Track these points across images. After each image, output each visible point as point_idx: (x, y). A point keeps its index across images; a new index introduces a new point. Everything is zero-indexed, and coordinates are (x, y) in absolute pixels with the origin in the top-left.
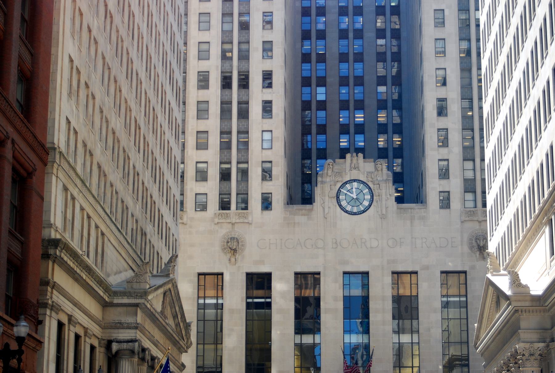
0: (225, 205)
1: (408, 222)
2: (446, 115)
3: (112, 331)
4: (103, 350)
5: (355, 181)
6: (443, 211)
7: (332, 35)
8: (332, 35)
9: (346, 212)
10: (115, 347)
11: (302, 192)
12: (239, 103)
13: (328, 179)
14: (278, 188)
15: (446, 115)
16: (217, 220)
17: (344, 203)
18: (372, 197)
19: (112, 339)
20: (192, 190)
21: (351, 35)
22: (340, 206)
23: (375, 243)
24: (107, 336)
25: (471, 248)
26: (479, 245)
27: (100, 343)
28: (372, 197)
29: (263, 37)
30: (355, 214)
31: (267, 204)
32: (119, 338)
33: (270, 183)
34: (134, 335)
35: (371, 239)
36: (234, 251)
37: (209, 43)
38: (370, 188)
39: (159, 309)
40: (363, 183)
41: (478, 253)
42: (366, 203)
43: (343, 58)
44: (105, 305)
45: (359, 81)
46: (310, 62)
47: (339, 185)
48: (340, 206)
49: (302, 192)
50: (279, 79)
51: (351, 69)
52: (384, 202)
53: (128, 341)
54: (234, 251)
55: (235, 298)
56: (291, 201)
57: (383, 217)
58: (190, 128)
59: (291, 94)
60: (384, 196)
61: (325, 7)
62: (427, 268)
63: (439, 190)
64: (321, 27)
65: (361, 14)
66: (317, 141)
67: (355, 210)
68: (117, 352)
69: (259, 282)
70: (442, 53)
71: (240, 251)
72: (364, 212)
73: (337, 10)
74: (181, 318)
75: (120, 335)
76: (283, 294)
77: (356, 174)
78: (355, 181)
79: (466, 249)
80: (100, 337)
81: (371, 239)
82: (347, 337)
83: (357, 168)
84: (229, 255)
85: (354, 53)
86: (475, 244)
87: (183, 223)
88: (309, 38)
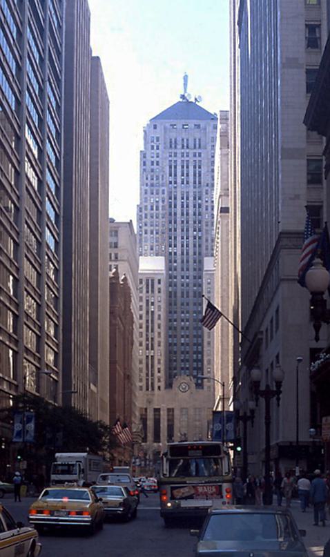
0: (147, 389)
11: (169, 385)
14: (162, 384)
36: (150, 402)
49: (169, 385)
54: (150, 402)
55: (150, 415)
56: (166, 388)
59: (166, 341)
69: (157, 410)
83: (184, 379)
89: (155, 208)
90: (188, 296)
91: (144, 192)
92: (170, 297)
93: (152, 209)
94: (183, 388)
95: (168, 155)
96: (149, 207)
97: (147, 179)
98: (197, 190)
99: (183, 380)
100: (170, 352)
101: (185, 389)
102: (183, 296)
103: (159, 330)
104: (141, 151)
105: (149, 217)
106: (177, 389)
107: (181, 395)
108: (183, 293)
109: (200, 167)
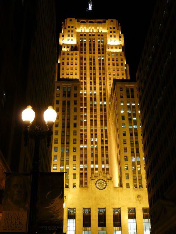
1: (117, 192)
2: (127, 161)
5: (101, 179)
15: (127, 161)
18: (106, 184)
21: (94, 143)
30: (101, 189)
31: (74, 186)
38: (105, 182)
40: (104, 180)
41: (138, 201)
42: (104, 186)
62: (123, 206)
67: (101, 188)
72: (104, 189)
78: (101, 179)
79: (135, 200)
82: (99, 228)
101: (102, 186)
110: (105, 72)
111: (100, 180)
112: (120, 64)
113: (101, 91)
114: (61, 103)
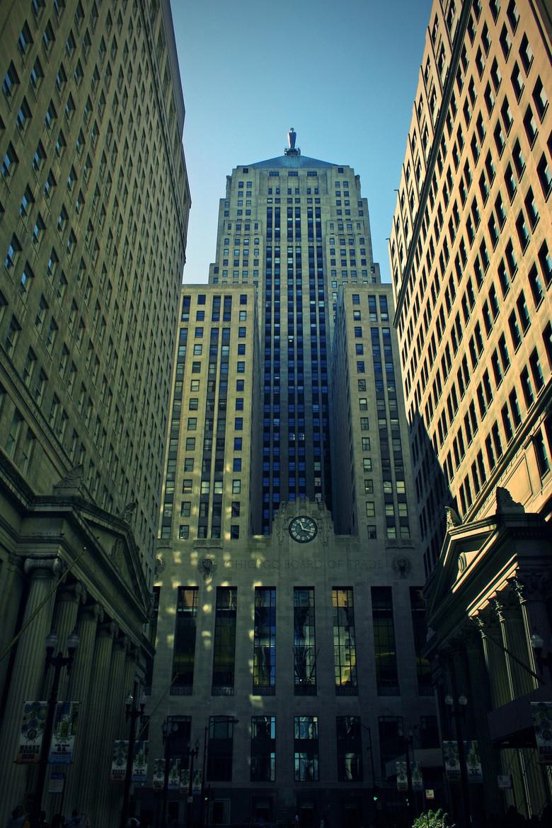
3: (30, 545)
4: (14, 568)
5: (303, 517)
6: (371, 540)
7: (284, 444)
8: (284, 444)
9: (297, 540)
10: (28, 563)
12: (216, 460)
13: (283, 516)
14: (243, 522)
16: (195, 546)
17: (294, 534)
19: (28, 554)
20: (177, 523)
22: (292, 536)
23: (318, 564)
24: (20, 550)
25: (394, 568)
26: (400, 566)
27: (10, 558)
28: (316, 530)
29: (236, 415)
32: (36, 554)
33: (238, 518)
34: (55, 550)
35: (315, 561)
37: (196, 418)
38: (314, 523)
39: (109, 551)
40: (309, 518)
41: (400, 573)
43: (292, 459)
44: (24, 514)
45: (302, 474)
46: (269, 461)
47: (291, 520)
48: (292, 536)
49: (262, 523)
50: (247, 405)
51: (297, 467)
52: (325, 533)
53: (46, 558)
57: (325, 544)
58: (179, 477)
60: (325, 528)
61: (279, 427)
63: (367, 524)
64: (276, 439)
65: (304, 432)
66: (272, 498)
67: (303, 539)
68: (33, 569)
70: (366, 427)
71: (212, 570)
73: (287, 428)
74: (140, 580)
75: (38, 550)
76: (247, 610)
77: (304, 513)
80: (11, 551)
81: (315, 561)
83: (305, 507)
84: (203, 573)
85: (299, 472)
86: (397, 565)
87: (169, 548)
88: (269, 492)
89: (241, 263)
90: (301, 401)
91: (223, 242)
92: (267, 401)
93: (236, 264)
94: (301, 532)
95: (266, 201)
96: (231, 262)
97: (230, 228)
98: (315, 244)
99: (304, 513)
100: (267, 430)
102: (291, 401)
103: (239, 395)
104: (221, 200)
105: (230, 275)
106: (284, 534)
107: (295, 548)
108: (291, 396)
109: (318, 216)
110: (325, 282)
111: (300, 518)
112: (359, 263)
113: (313, 325)
114: (207, 333)
